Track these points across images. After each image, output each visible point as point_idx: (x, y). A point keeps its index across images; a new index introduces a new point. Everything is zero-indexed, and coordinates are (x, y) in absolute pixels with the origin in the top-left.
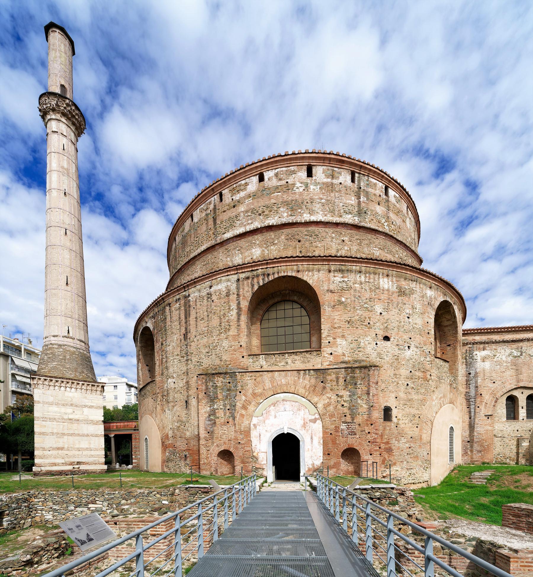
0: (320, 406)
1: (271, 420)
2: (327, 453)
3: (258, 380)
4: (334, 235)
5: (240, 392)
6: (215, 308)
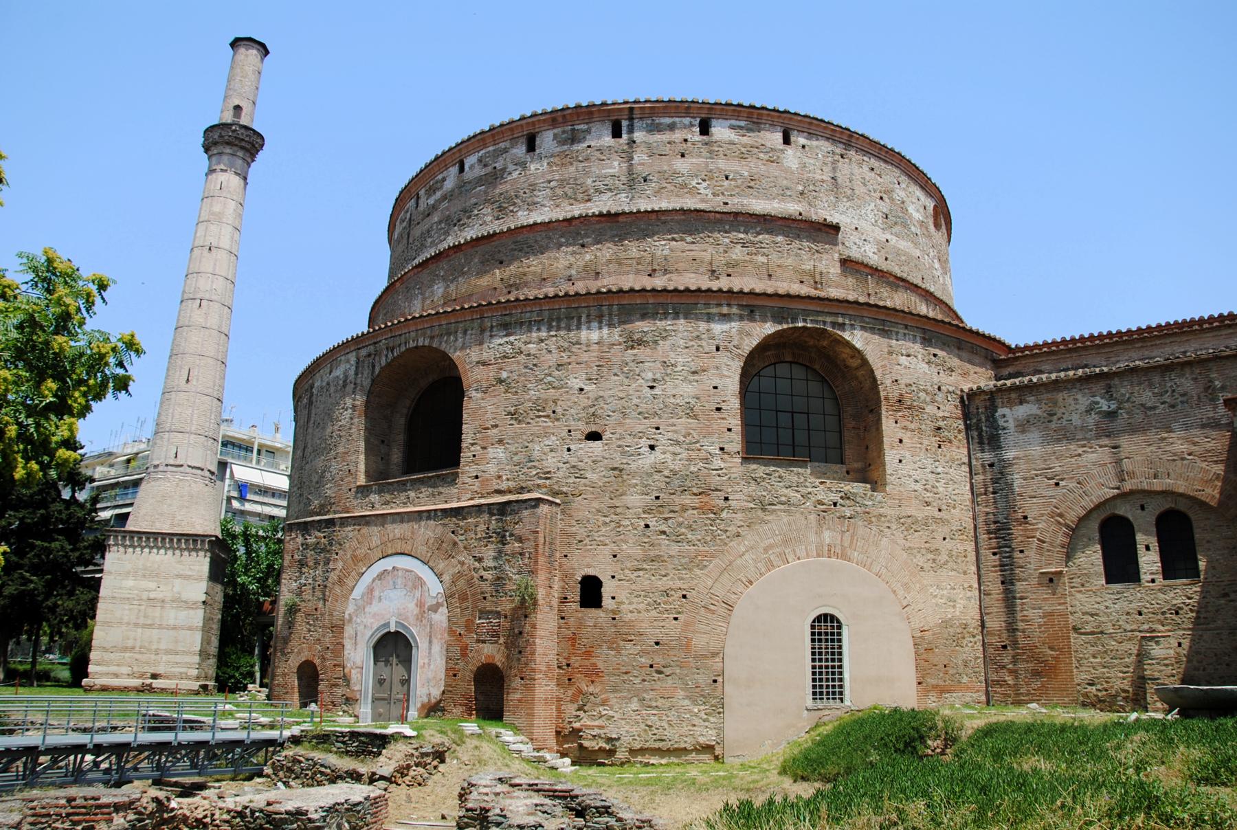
0: (446, 578)
1: (375, 608)
2: (452, 673)
3: (362, 531)
4: (563, 240)
5: (337, 554)
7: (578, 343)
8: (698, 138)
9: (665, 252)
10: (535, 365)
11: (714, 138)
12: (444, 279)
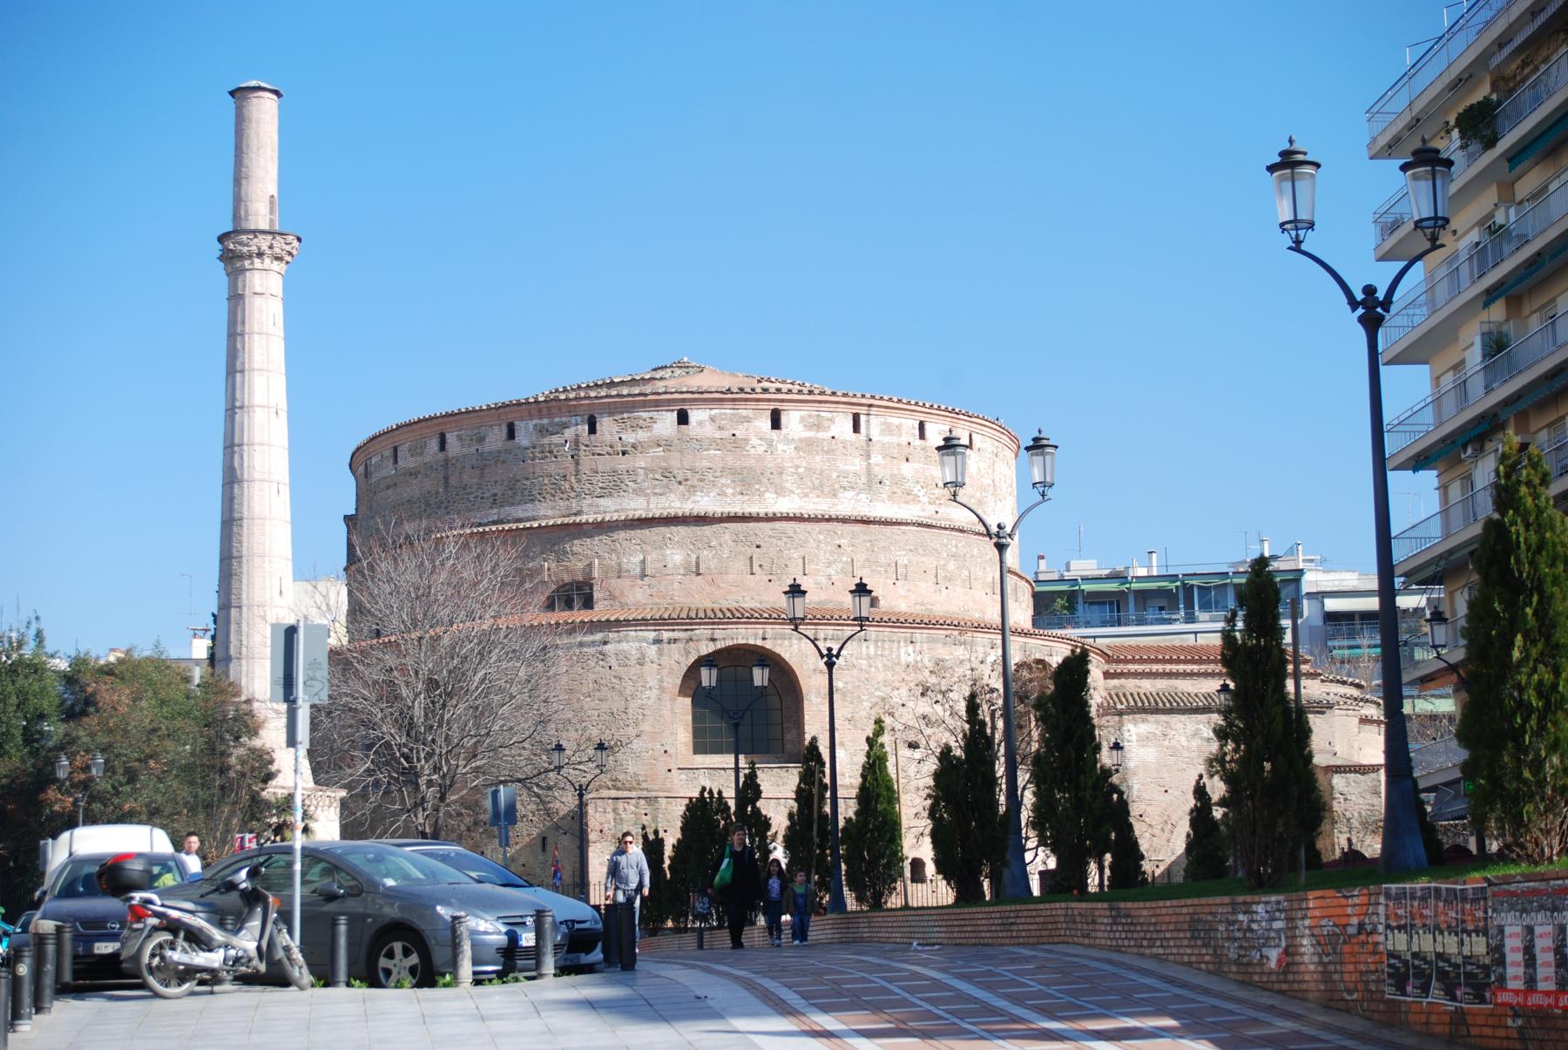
4: (821, 537)
6: (614, 680)
7: (899, 664)
8: (918, 442)
9: (906, 562)
10: (867, 679)
12: (680, 545)
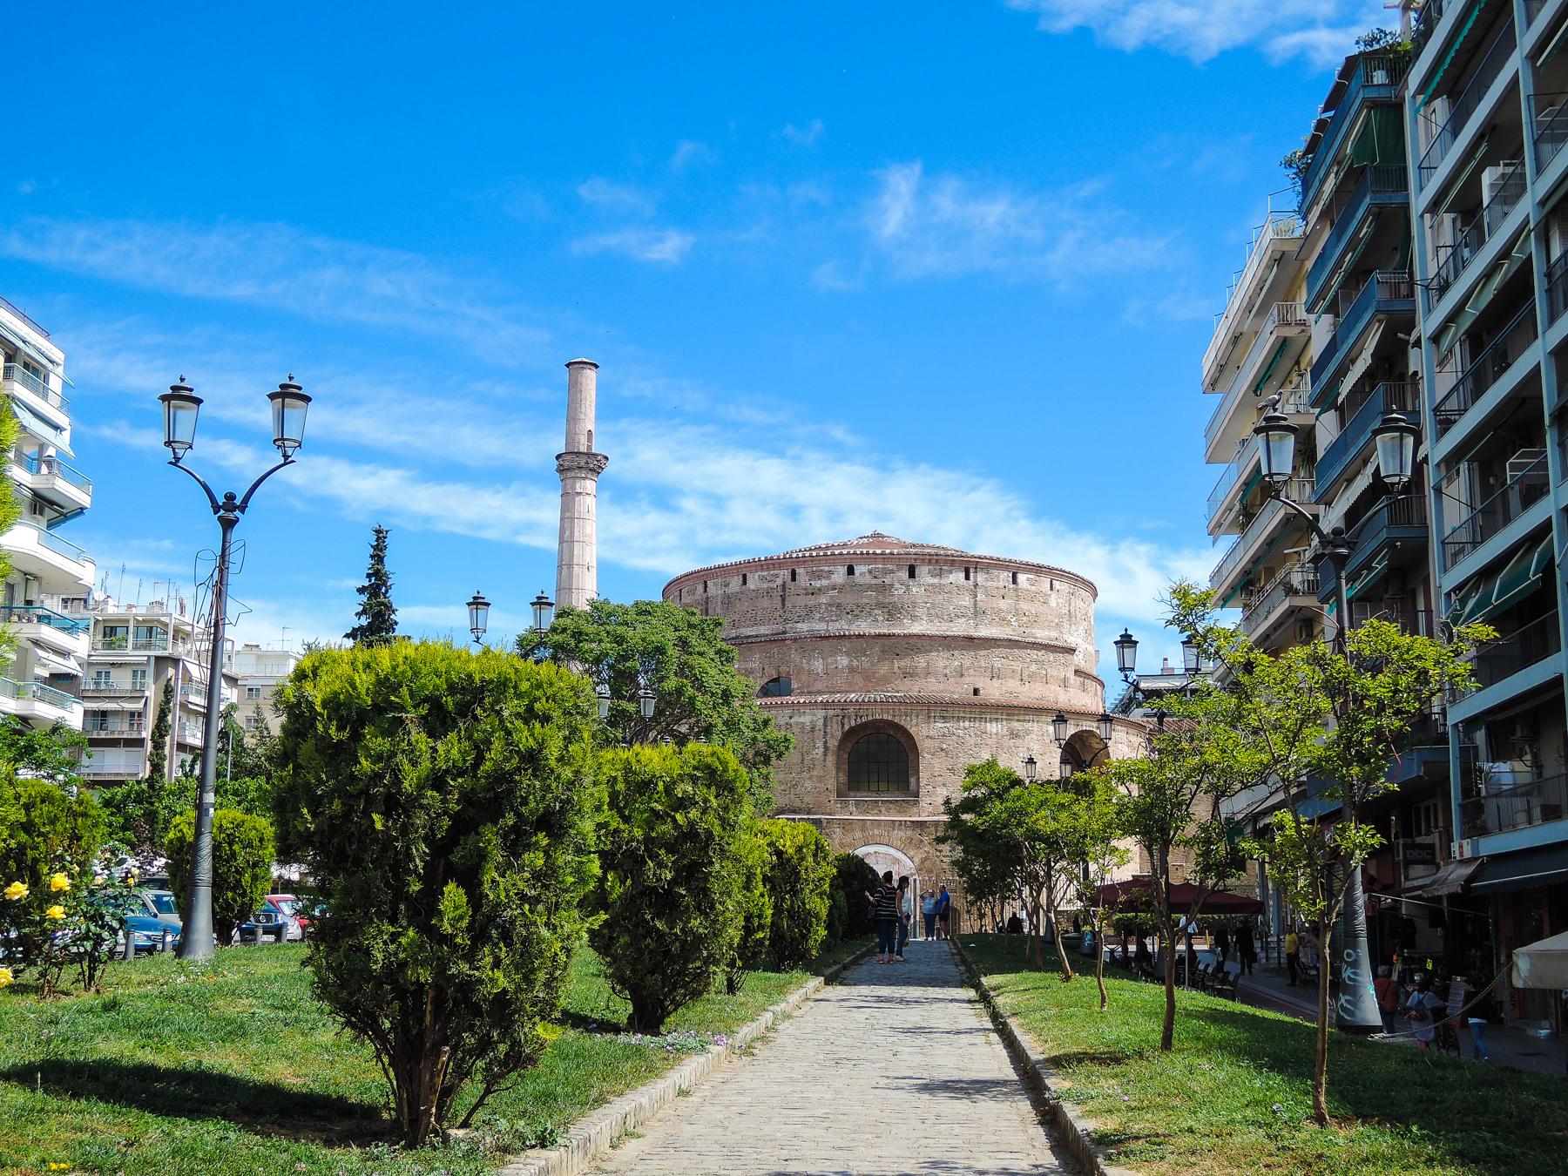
0: (916, 860)
8: (1012, 586)
11: (1020, 586)
12: (847, 654)
